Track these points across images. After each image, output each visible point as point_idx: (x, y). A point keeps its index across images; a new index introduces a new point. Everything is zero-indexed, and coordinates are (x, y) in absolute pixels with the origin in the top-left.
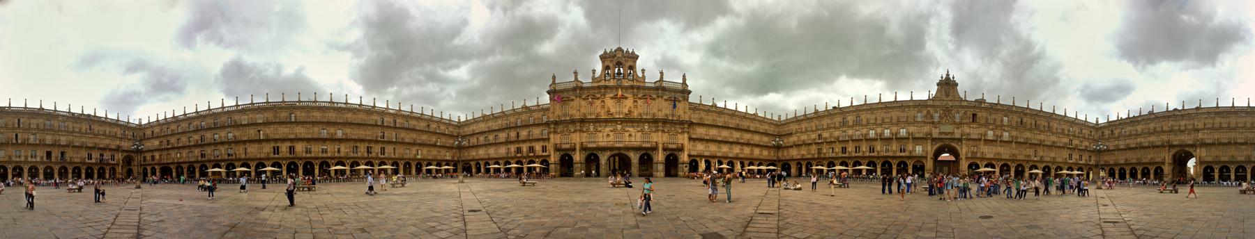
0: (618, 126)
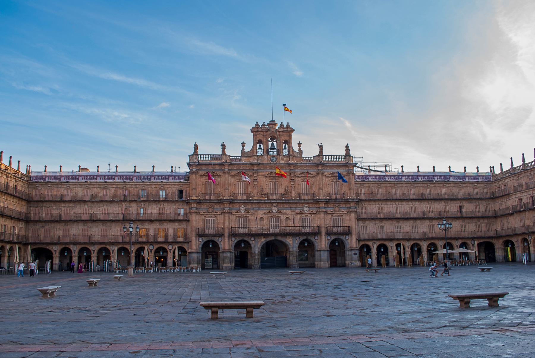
0: (274, 208)
